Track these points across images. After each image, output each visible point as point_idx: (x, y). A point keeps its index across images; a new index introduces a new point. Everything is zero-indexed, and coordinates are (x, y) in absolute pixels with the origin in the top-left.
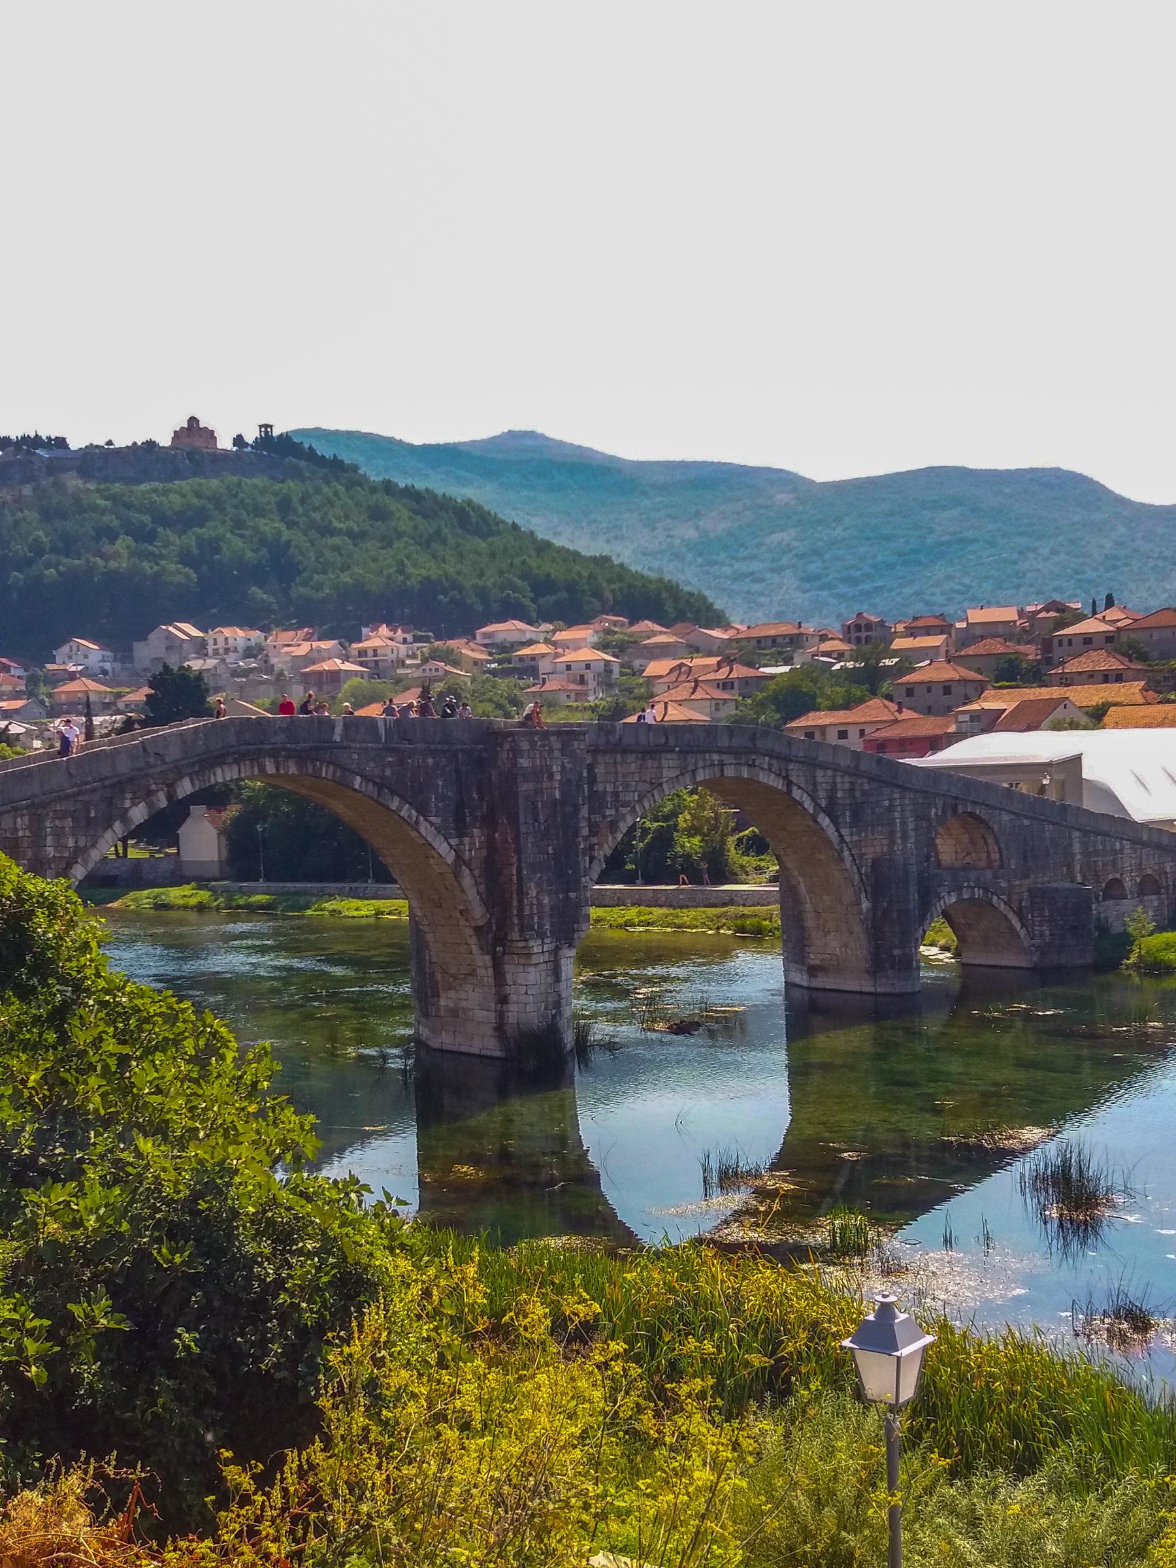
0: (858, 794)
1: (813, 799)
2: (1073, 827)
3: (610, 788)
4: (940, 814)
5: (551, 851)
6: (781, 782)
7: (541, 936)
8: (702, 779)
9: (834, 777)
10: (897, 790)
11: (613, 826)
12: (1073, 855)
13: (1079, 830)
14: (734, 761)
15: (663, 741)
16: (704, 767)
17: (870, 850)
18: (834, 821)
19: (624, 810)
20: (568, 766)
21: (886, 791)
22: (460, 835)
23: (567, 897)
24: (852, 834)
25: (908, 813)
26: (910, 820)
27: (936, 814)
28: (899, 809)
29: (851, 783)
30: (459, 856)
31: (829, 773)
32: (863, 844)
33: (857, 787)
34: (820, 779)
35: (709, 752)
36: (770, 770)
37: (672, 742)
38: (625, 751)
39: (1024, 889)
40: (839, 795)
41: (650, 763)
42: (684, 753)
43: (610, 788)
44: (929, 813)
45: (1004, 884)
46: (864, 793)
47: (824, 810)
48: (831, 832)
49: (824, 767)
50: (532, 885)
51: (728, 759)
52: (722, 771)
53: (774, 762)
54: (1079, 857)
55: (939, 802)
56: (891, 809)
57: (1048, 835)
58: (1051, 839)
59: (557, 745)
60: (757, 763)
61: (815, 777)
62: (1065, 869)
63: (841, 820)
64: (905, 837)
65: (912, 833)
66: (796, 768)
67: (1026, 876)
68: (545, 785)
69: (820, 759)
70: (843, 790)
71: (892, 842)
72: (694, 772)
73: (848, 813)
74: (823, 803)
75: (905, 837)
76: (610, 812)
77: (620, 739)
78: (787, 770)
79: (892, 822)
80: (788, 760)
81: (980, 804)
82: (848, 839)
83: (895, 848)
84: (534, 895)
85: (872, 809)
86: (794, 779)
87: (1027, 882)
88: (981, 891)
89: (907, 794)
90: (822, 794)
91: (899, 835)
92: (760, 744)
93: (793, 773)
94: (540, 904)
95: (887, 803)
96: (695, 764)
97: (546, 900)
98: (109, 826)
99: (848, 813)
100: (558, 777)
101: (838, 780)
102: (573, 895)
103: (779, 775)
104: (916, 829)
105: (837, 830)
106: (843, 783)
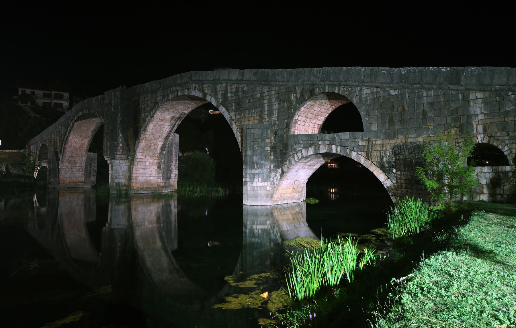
0: (240, 94)
1: (216, 99)
2: (469, 90)
4: (298, 97)
5: (110, 128)
6: (201, 94)
7: (107, 155)
8: (170, 98)
9: (226, 86)
10: (265, 87)
12: (469, 117)
13: (484, 91)
14: (181, 89)
16: (171, 93)
18: (227, 109)
19: (147, 114)
20: (116, 101)
23: (114, 143)
24: (236, 115)
25: (274, 99)
26: (275, 103)
27: (296, 97)
28: (267, 98)
29: (237, 88)
32: (242, 120)
33: (240, 89)
34: (218, 89)
35: (172, 87)
39: (388, 147)
40: (229, 95)
43: (143, 107)
44: (290, 98)
45: (360, 143)
46: (243, 91)
47: (221, 104)
50: (106, 139)
51: (179, 88)
52: (177, 94)
54: (481, 117)
55: (299, 90)
56: (262, 98)
57: (425, 100)
58: (431, 104)
59: (113, 95)
60: (190, 87)
61: (216, 88)
62: (453, 131)
63: (230, 108)
65: (277, 112)
66: (207, 86)
68: (110, 108)
69: (221, 79)
70: (231, 93)
71: (261, 117)
72: (168, 95)
73: (234, 104)
74: (220, 102)
75: (270, 114)
76: (143, 115)
77: (147, 88)
78: (203, 88)
79: (262, 106)
81: (339, 85)
82: (234, 118)
83: (264, 121)
84: (106, 142)
85: (249, 100)
86: (206, 92)
87: (392, 142)
88: (339, 149)
89: (274, 88)
90: (220, 96)
91: (266, 113)
93: (206, 88)
94: (107, 145)
95: (259, 95)
96: (168, 92)
97: (108, 144)
98: (68, 128)
99: (234, 104)
101: (229, 87)
102: (115, 143)
103: (200, 91)
105: (229, 112)
106: (231, 89)
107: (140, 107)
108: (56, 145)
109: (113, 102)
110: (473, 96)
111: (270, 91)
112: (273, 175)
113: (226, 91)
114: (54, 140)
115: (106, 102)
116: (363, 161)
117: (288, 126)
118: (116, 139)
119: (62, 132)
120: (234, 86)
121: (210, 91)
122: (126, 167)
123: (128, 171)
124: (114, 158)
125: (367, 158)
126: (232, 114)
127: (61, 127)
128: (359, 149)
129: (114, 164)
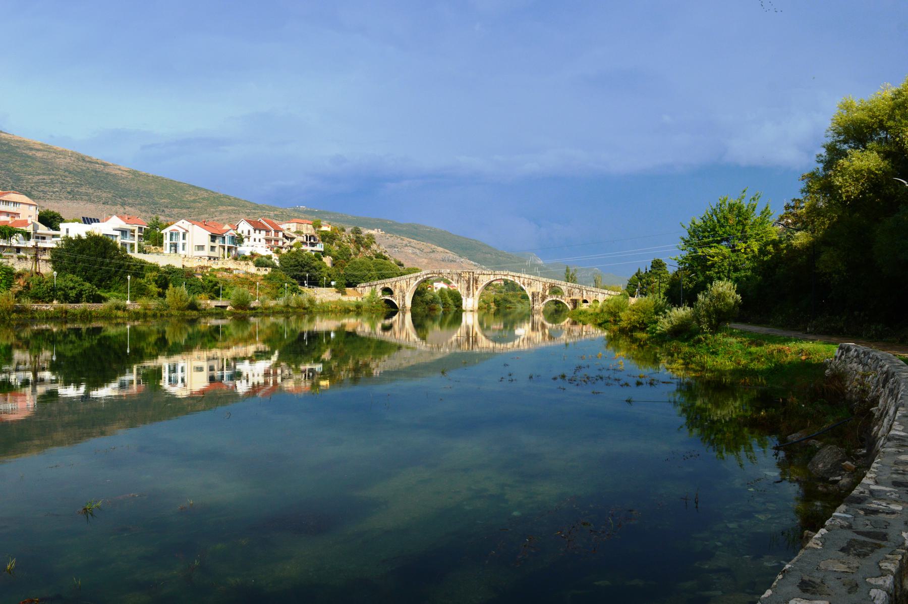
1: (520, 281)
11: (482, 284)
21: (536, 282)
38: (484, 274)
40: (525, 282)
42: (494, 275)
49: (522, 277)
55: (548, 284)
64: (540, 289)
67: (570, 297)
71: (537, 289)
74: (522, 283)
75: (540, 289)
76: (481, 282)
80: (514, 276)
100: (467, 277)
113: (524, 280)
115: (462, 275)
117: (545, 292)
118: (470, 290)
120: (527, 280)
124: (468, 297)
126: (526, 287)
127: (408, 280)
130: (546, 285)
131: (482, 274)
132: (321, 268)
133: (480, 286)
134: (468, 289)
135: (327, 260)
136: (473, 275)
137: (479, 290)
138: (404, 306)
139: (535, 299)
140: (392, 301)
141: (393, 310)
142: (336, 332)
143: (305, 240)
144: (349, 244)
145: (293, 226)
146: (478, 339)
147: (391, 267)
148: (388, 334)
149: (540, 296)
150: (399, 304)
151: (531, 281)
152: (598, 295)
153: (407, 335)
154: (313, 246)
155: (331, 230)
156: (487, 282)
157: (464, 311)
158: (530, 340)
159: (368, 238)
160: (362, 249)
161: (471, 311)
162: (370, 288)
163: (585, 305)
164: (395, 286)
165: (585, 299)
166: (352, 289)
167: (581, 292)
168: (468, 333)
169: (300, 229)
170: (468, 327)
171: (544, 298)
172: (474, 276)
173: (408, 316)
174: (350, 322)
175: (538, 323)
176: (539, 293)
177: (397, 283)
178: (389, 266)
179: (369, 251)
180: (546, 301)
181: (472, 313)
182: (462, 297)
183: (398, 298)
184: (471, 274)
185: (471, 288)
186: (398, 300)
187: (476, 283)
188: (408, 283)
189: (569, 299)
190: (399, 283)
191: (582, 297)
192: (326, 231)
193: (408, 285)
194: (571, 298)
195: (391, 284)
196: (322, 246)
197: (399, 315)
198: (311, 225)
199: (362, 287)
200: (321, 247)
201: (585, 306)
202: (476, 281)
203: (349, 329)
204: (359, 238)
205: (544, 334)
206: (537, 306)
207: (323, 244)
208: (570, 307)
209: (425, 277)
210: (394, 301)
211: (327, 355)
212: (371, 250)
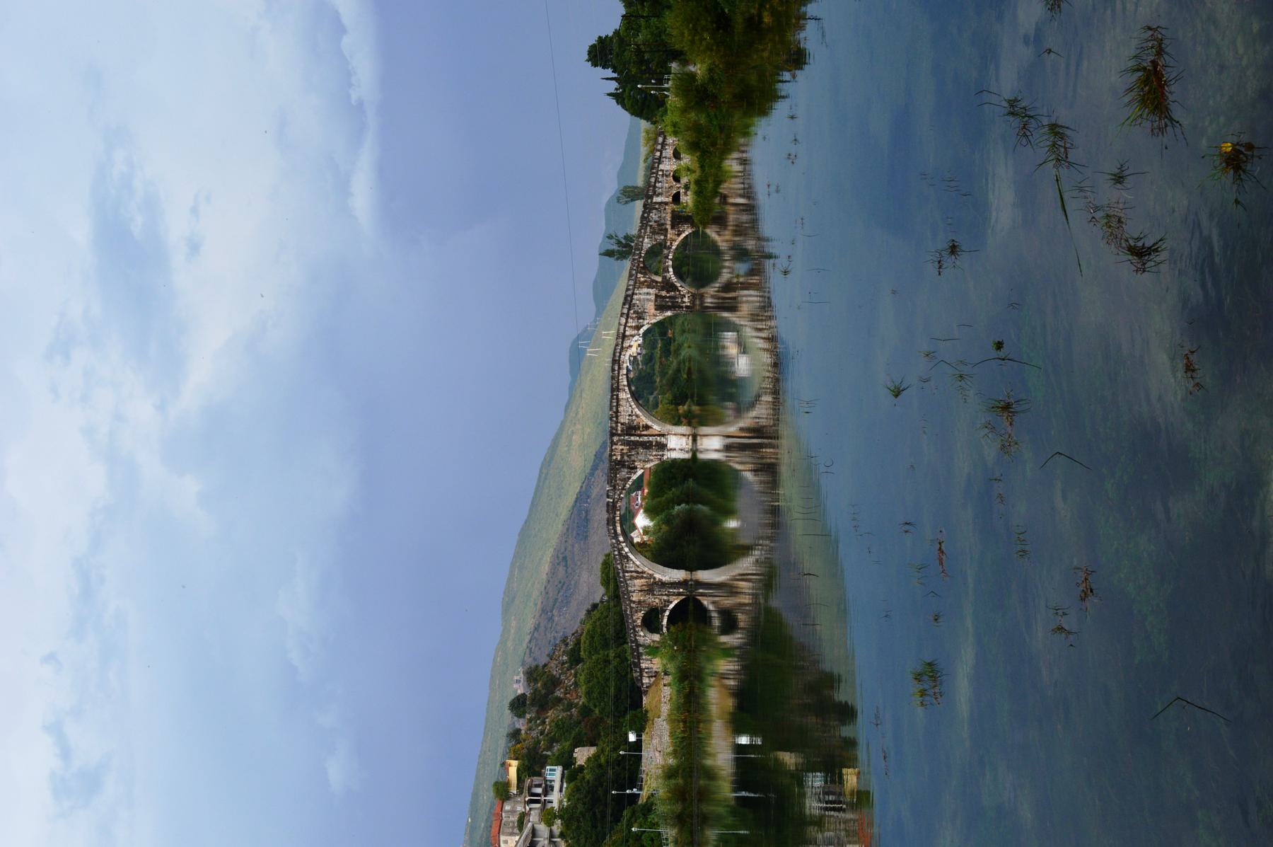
3: (627, 418)
7: (663, 455)
9: (629, 327)
15: (615, 397)
17: (653, 311)
18: (643, 326)
19: (634, 413)
21: (634, 302)
22: (637, 468)
30: (642, 469)
31: (627, 329)
35: (618, 379)
36: (624, 355)
37: (615, 393)
40: (634, 325)
41: (621, 403)
42: (618, 389)
43: (627, 418)
48: (645, 328)
49: (625, 331)
51: (621, 374)
53: (623, 353)
55: (639, 275)
56: (639, 300)
62: (667, 207)
64: (648, 294)
67: (666, 230)
72: (624, 386)
74: (636, 332)
75: (648, 294)
77: (614, 412)
79: (644, 300)
80: (622, 347)
82: (648, 321)
87: (669, 230)
89: (635, 291)
92: (617, 358)
94: (655, 455)
97: (654, 453)
100: (623, 447)
104: (648, 288)
107: (627, 421)
108: (646, 588)
109: (621, 447)
110: (654, 201)
111: (636, 294)
112: (682, 293)
113: (631, 327)
114: (640, 594)
116: (676, 243)
117: (657, 282)
119: (632, 572)
121: (629, 341)
122: (674, 437)
123: (677, 436)
125: (675, 241)
126: (646, 322)
127: (627, 574)
128: (671, 243)
129: (671, 447)
130: (642, 279)
131: (617, 417)
132: (600, 766)
133: (644, 420)
134: (647, 446)
135: (582, 755)
136: (619, 435)
137: (650, 423)
138: (683, 584)
139: (670, 304)
140: (672, 611)
141: (691, 604)
142: (738, 731)
143: (538, 806)
144: (547, 720)
145: (506, 842)
146: (753, 425)
147: (599, 619)
148: (742, 618)
149: (664, 293)
150: (679, 594)
151: (632, 312)
152: (662, 171)
153: (743, 577)
154: (552, 788)
155: (516, 760)
156: (634, 406)
157: (694, 455)
158: (758, 315)
159: (536, 681)
160: (559, 693)
161: (694, 440)
162: (644, 657)
163: (683, 199)
164: (640, 602)
165: (670, 199)
166: (644, 698)
167: (657, 206)
168: (742, 448)
169: (513, 828)
170: (728, 448)
171: (668, 286)
172: (619, 432)
173: (704, 575)
174: (717, 700)
175: (719, 298)
176: (657, 296)
177: (634, 599)
178: (598, 623)
179: (563, 677)
180: (674, 279)
181: (698, 438)
182: (665, 457)
183: (665, 598)
184: (615, 439)
185: (646, 439)
186: (671, 598)
187: (637, 428)
188: (634, 574)
189: (671, 233)
190: (634, 594)
191: (666, 204)
192: (518, 770)
193: (640, 574)
194: (669, 227)
195: (636, 612)
196: (551, 770)
197: (702, 595)
198: (505, 804)
199: (641, 676)
200: (554, 770)
201: (688, 199)
202: (631, 429)
203: (730, 703)
204: (533, 700)
205: (746, 286)
206: (686, 300)
207: (548, 767)
208: (688, 231)
209: (621, 539)
210: (671, 606)
211: (789, 759)
212: (560, 674)
